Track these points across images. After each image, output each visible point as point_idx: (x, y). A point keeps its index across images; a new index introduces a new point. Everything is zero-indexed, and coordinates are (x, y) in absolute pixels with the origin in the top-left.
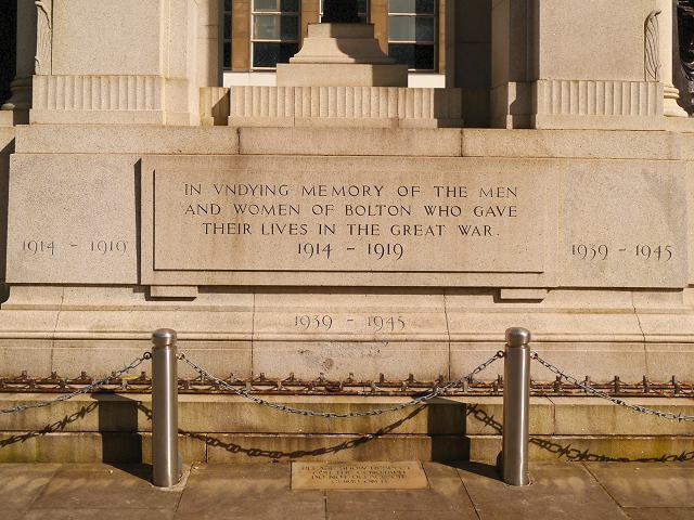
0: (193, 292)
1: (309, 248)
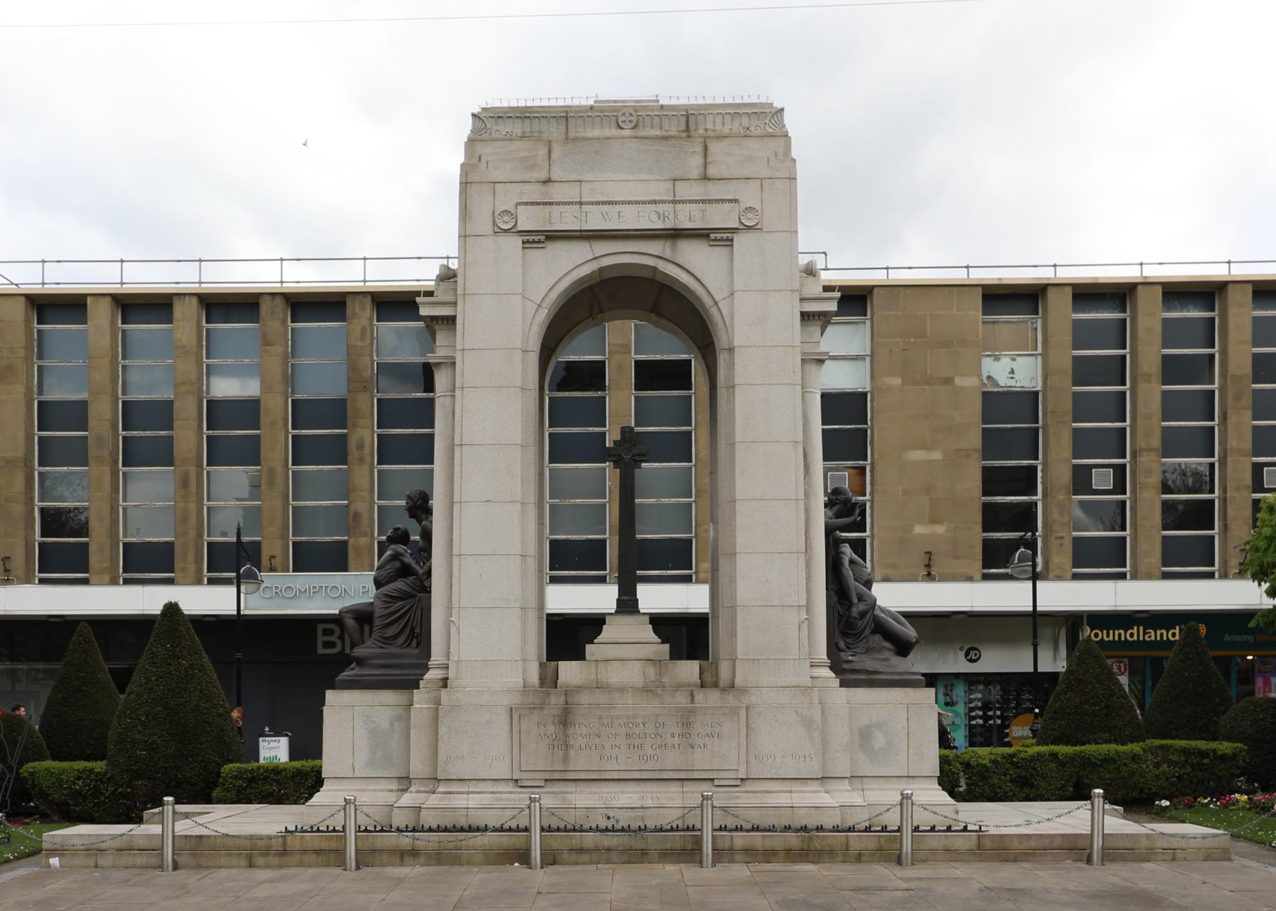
0: (542, 784)
1: (606, 758)
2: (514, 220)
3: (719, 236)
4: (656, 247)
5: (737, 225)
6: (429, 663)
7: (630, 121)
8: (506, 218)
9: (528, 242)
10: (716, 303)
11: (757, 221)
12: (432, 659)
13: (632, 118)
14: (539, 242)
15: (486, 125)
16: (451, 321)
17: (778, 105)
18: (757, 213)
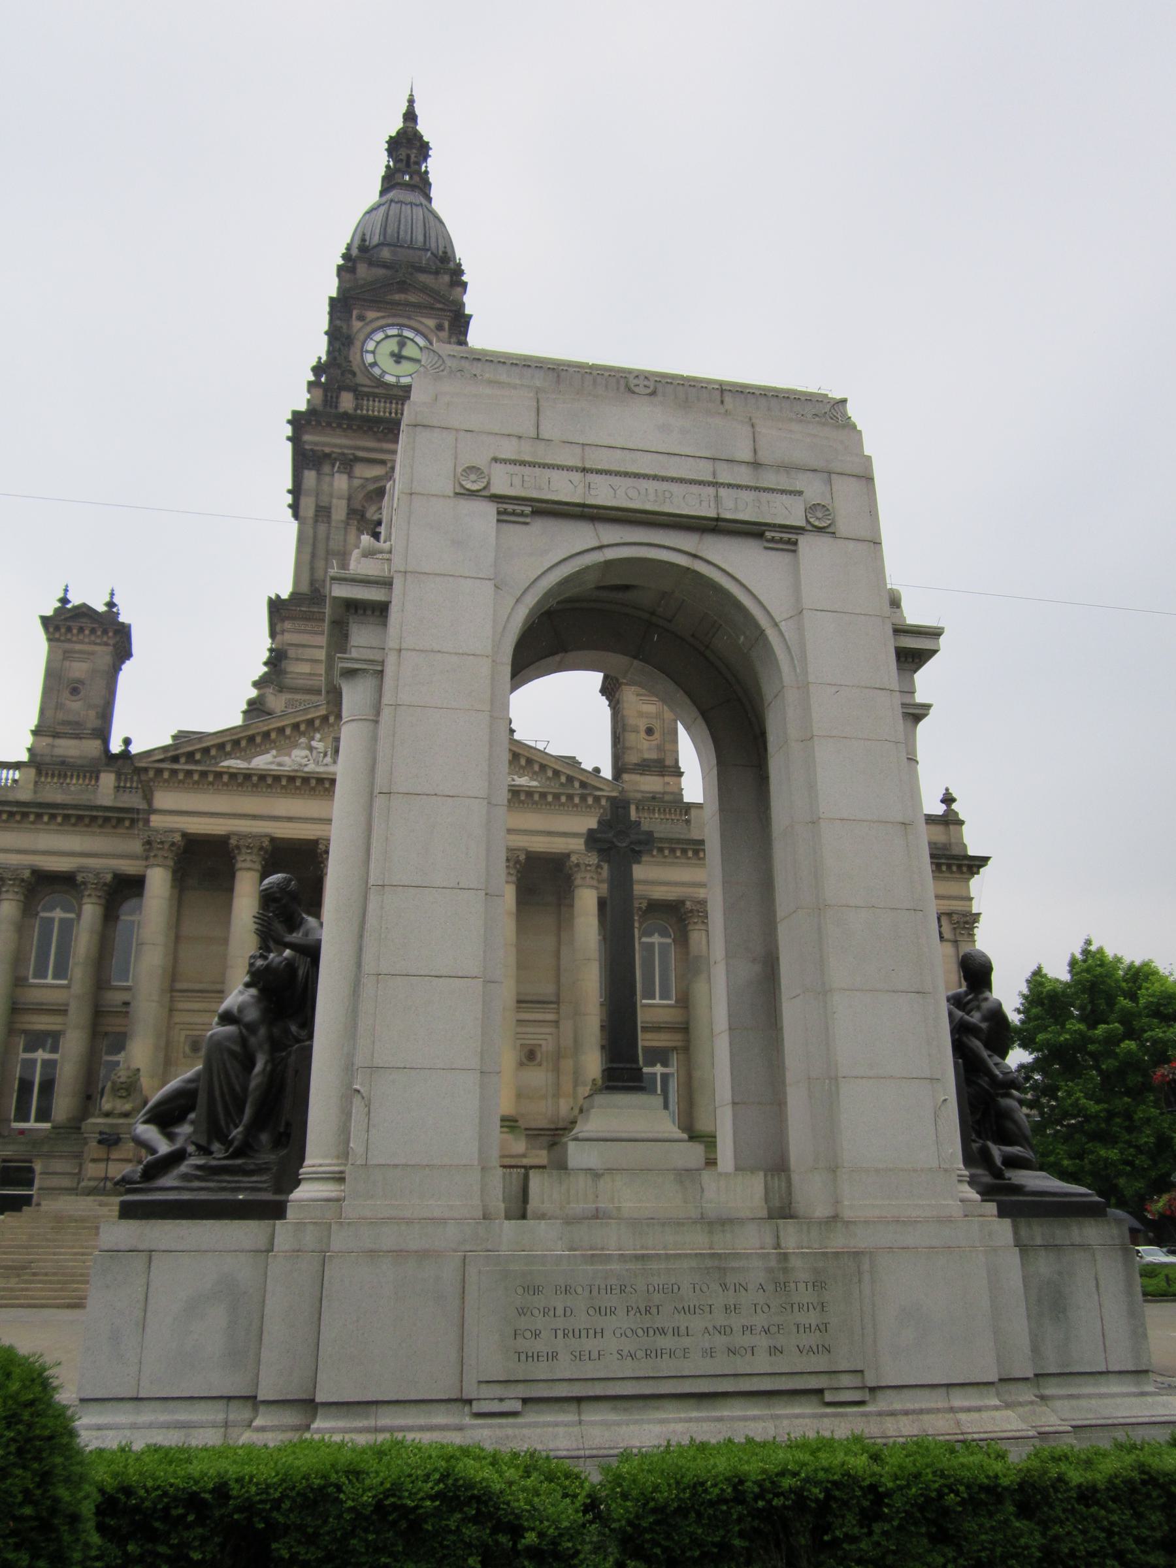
0: (517, 1406)
2: (485, 481)
3: (777, 535)
4: (687, 541)
5: (802, 523)
6: (302, 1171)
7: (645, 386)
8: (473, 477)
9: (505, 512)
10: (776, 625)
11: (829, 522)
12: (307, 1162)
13: (646, 383)
14: (522, 514)
15: (444, 361)
16: (381, 610)
17: (837, 395)
18: (827, 513)
